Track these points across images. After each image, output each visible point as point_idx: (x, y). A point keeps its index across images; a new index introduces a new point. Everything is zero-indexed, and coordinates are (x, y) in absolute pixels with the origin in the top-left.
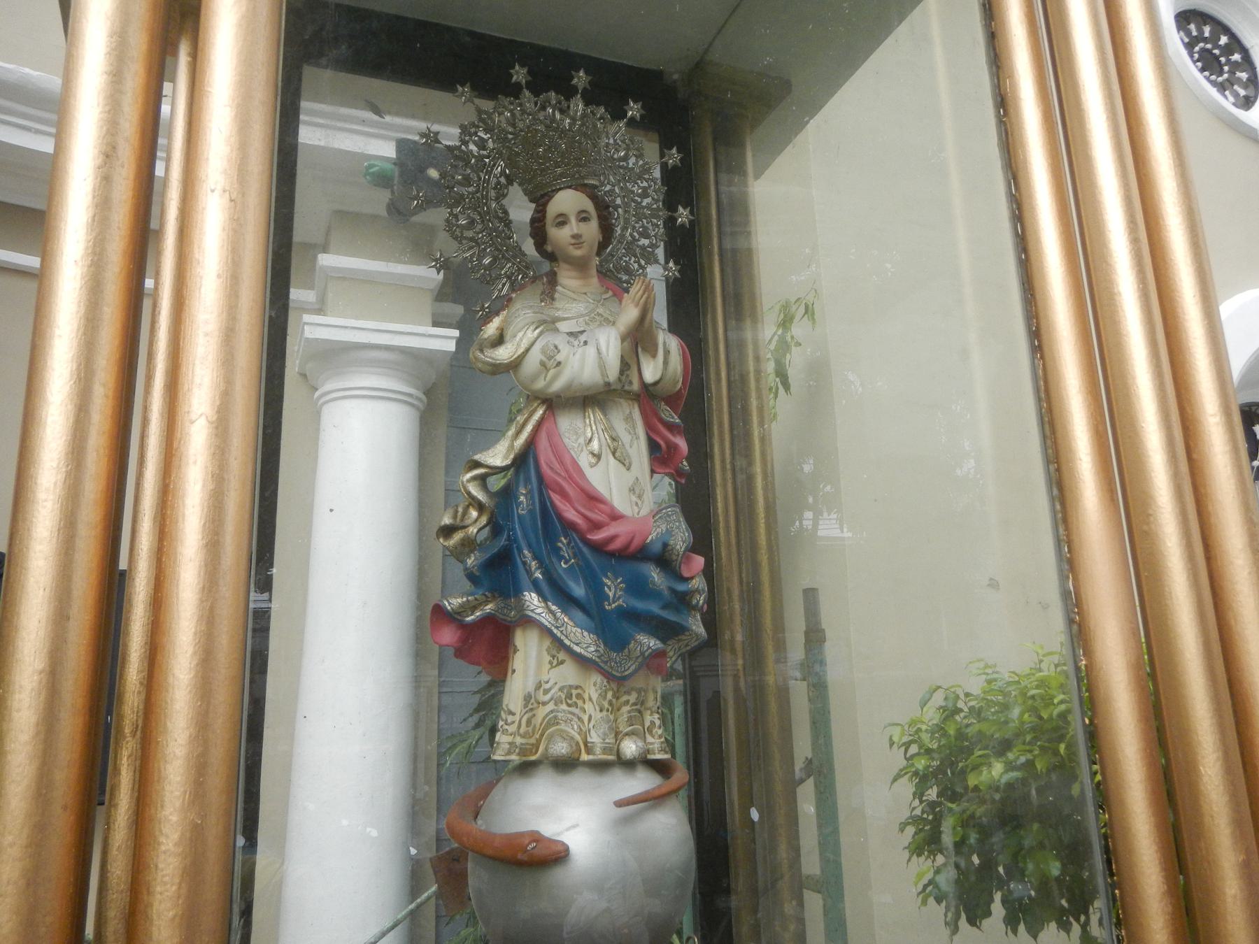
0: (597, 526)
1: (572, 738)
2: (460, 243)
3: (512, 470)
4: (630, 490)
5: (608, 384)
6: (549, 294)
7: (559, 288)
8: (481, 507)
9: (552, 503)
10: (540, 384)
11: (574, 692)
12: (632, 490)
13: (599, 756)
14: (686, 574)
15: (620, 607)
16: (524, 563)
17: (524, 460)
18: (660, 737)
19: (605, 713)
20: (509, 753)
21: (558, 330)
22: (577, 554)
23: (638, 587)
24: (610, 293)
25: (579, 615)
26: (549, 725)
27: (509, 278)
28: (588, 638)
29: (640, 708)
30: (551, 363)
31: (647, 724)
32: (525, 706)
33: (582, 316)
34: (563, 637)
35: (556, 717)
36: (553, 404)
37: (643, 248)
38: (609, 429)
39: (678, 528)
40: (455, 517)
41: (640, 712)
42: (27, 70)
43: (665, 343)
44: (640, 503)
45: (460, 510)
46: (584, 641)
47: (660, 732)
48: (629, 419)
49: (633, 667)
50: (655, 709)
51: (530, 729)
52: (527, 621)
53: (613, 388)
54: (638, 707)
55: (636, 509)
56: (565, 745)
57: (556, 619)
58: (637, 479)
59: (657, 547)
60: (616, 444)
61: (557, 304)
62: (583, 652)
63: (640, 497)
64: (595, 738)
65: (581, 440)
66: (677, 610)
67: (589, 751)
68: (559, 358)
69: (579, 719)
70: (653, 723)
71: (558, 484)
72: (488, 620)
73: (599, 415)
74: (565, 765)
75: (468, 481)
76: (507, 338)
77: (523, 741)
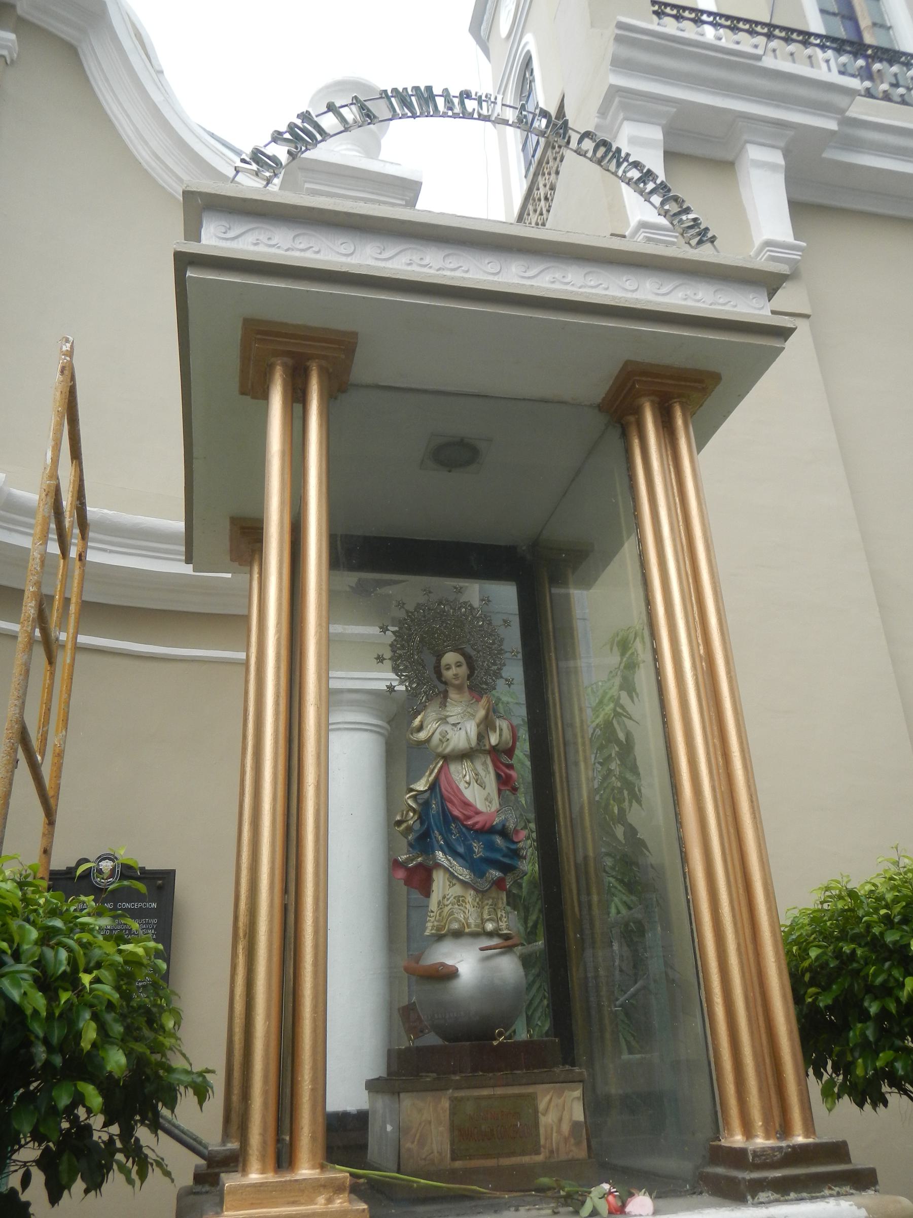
0: (469, 818)
1: (461, 921)
2: (400, 678)
3: (429, 792)
4: (485, 799)
5: (471, 748)
6: (443, 705)
7: (448, 700)
8: (414, 811)
9: (448, 808)
10: (440, 750)
11: (461, 899)
12: (486, 799)
13: (473, 928)
14: (516, 840)
15: (481, 856)
16: (435, 837)
17: (434, 786)
18: (506, 922)
19: (475, 908)
20: (432, 930)
21: (448, 723)
22: (460, 832)
23: (491, 846)
24: (474, 700)
25: (461, 860)
26: (450, 915)
27: (425, 693)
28: (466, 872)
29: (495, 908)
30: (444, 740)
31: (499, 916)
32: (438, 907)
33: (460, 714)
34: (454, 872)
35: (452, 911)
36: (447, 758)
37: (494, 672)
38: (474, 770)
39: (511, 817)
40: (402, 816)
41: (495, 909)
42: (105, 511)
43: (499, 726)
44: (490, 805)
45: (405, 812)
46: (464, 873)
47: (505, 919)
48: (484, 764)
49: (489, 886)
50: (502, 908)
51: (441, 918)
52: (438, 866)
53: (475, 749)
54: (493, 906)
55: (489, 809)
56: (457, 924)
57: (451, 863)
58: (489, 794)
59: (500, 827)
60: (477, 777)
61: (448, 709)
62: (463, 878)
63: (490, 802)
64: (471, 921)
65: (461, 776)
66: (511, 858)
67: (469, 926)
68: (448, 737)
69: (464, 912)
70: (502, 915)
71: (450, 798)
72: (420, 865)
73: (470, 763)
74: (458, 934)
75: (408, 798)
76: (424, 727)
77: (438, 924)
